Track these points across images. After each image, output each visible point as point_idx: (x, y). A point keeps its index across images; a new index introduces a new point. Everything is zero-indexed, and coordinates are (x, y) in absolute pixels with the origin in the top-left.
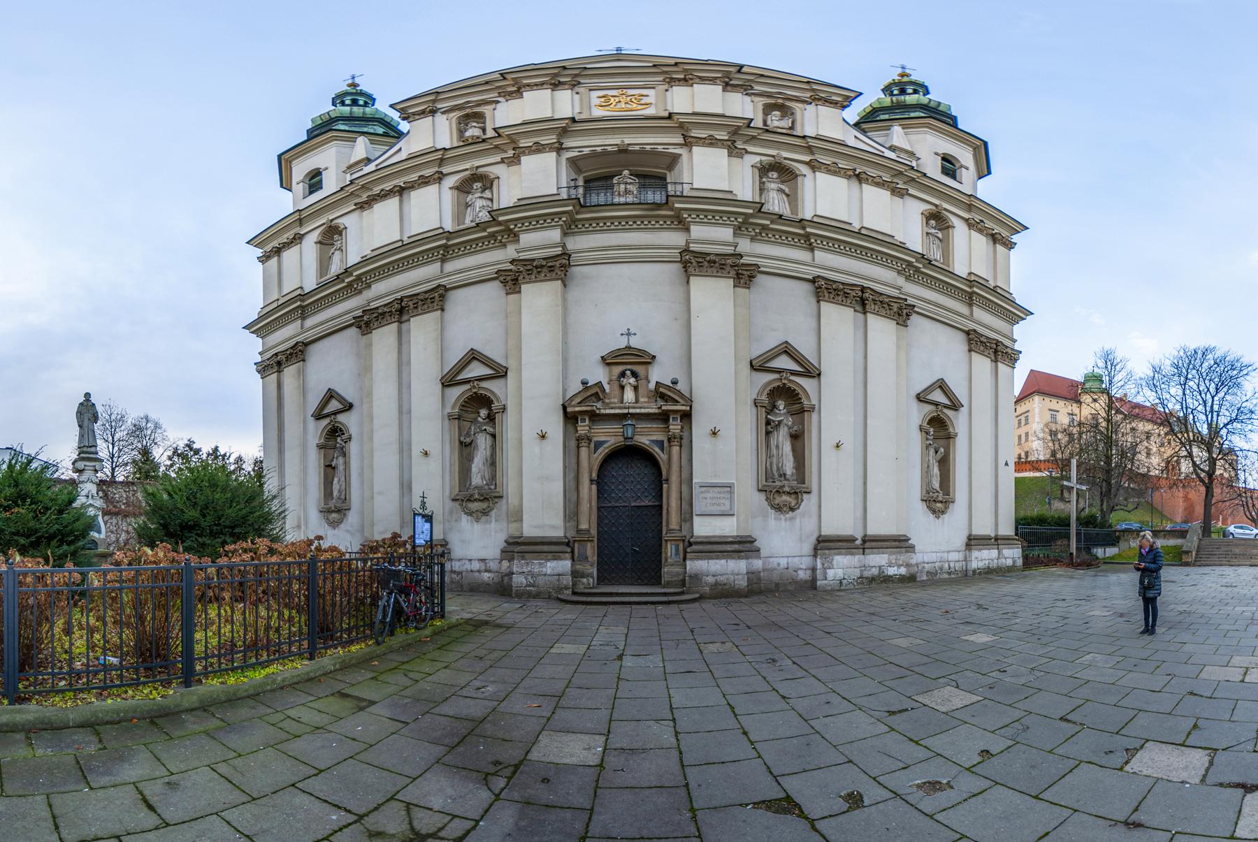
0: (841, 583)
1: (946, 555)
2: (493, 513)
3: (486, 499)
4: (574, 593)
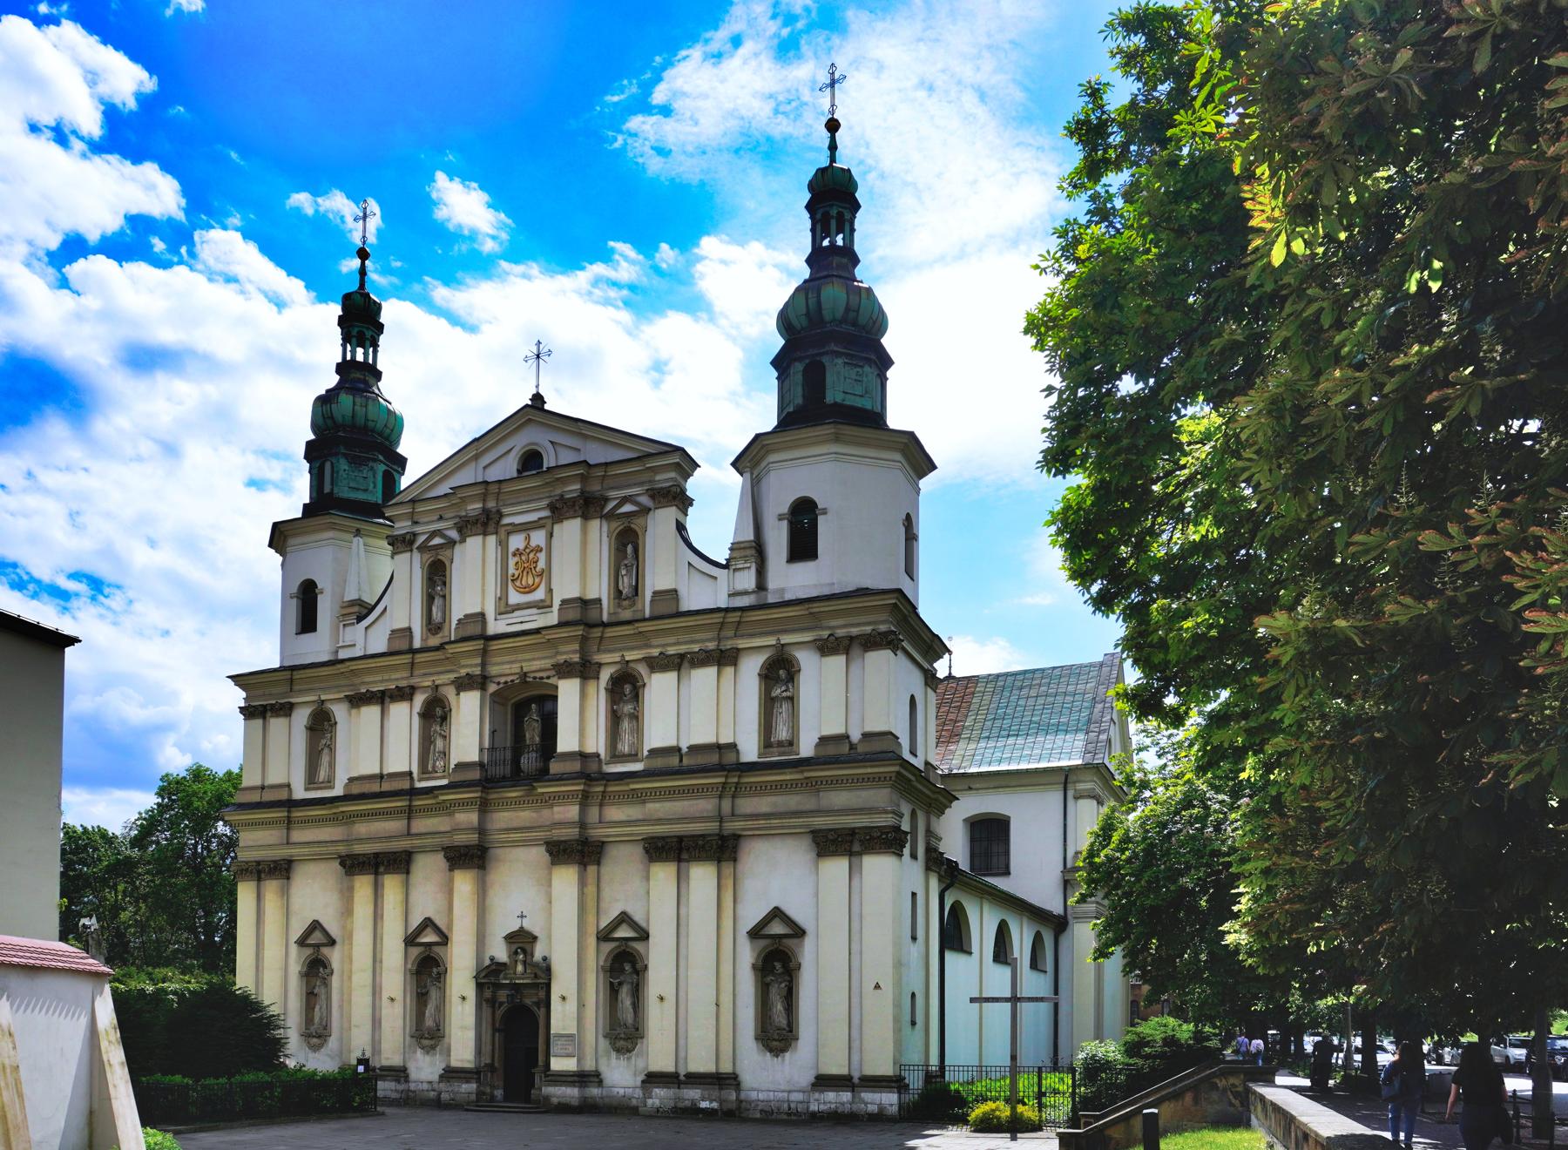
0: (658, 1111)
1: (786, 1094)
2: (438, 1049)
3: (432, 1038)
4: (477, 1106)
